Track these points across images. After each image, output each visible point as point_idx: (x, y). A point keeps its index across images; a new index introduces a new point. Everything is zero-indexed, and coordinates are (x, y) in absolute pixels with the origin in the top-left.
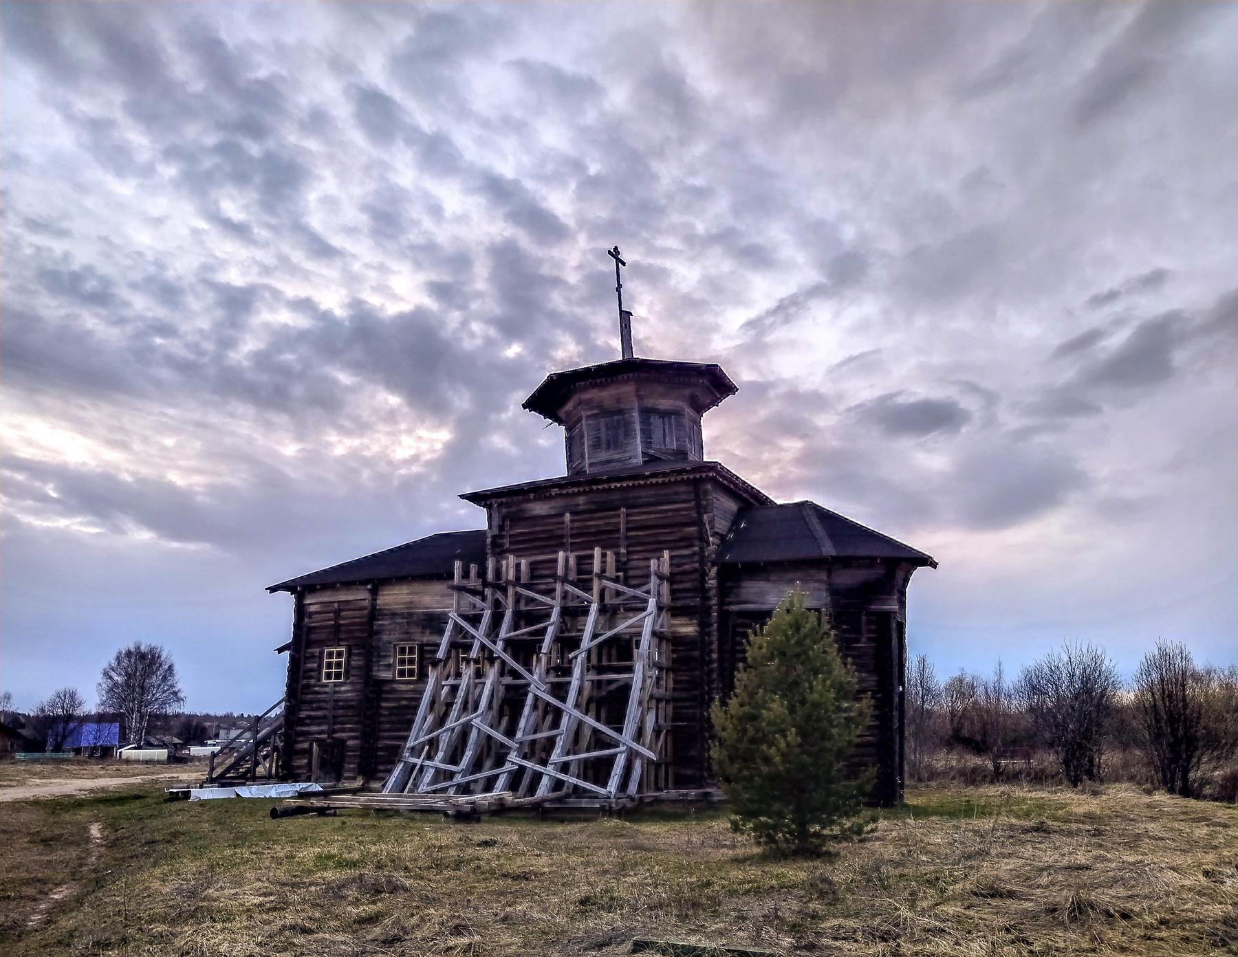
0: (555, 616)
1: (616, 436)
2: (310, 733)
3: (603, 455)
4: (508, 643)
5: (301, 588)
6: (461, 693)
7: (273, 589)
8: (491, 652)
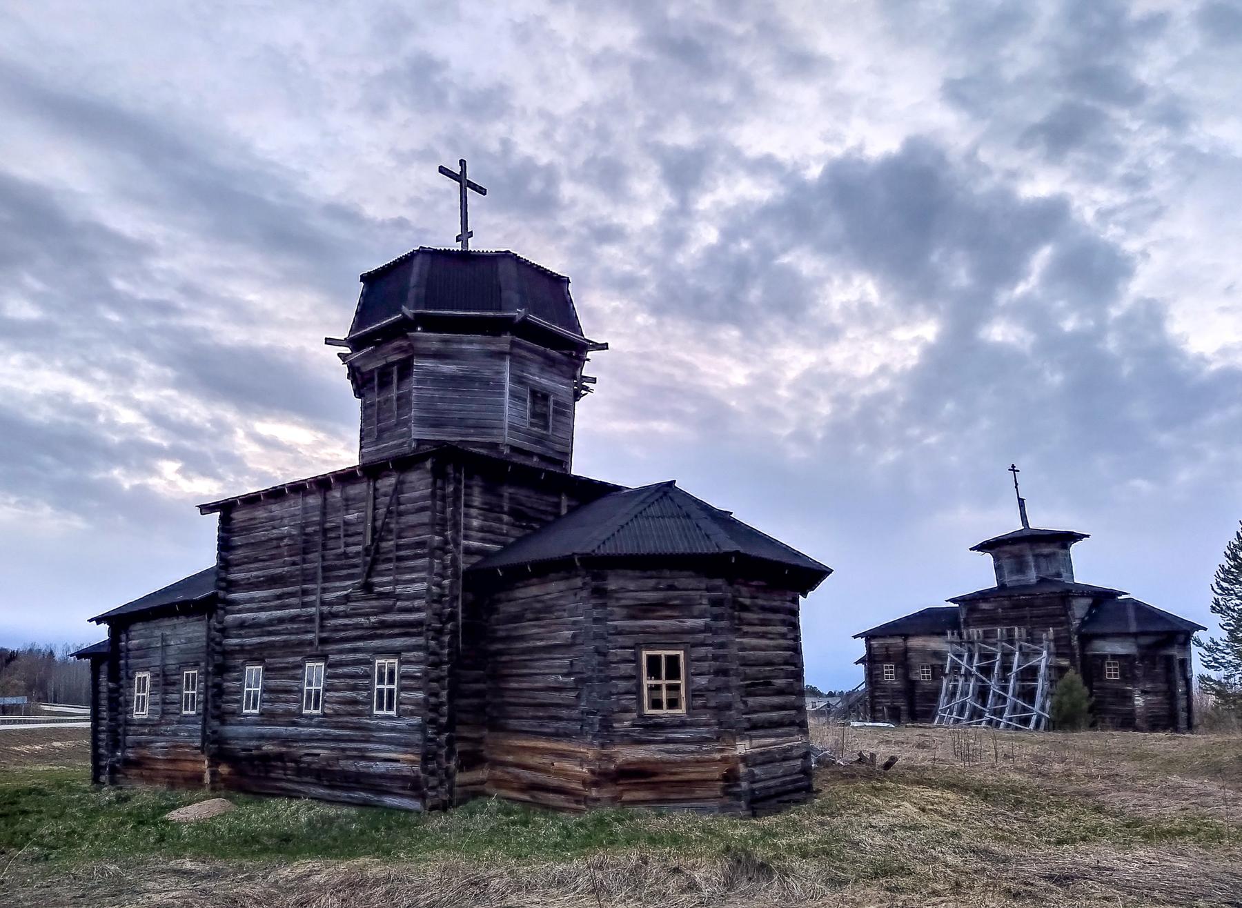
0: (998, 657)
1: (1021, 568)
2: (882, 702)
3: (1015, 578)
4: (980, 669)
5: (869, 636)
6: (960, 688)
7: (855, 637)
8: (970, 672)
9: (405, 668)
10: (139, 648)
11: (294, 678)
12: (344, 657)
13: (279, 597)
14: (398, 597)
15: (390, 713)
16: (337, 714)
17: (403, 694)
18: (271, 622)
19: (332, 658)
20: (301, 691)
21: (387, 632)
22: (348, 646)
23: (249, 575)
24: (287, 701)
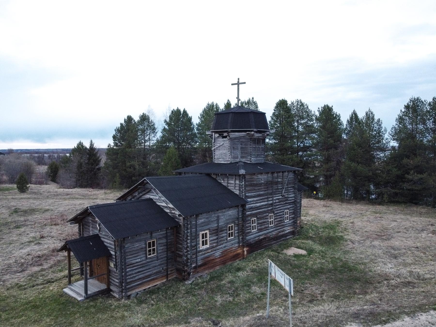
9: (290, 211)
10: (202, 223)
11: (266, 219)
12: (278, 212)
13: (261, 199)
14: (288, 198)
15: (288, 221)
16: (277, 224)
17: (290, 216)
18: (260, 206)
19: (276, 212)
20: (268, 221)
21: (286, 205)
22: (279, 209)
23: (252, 194)
24: (264, 225)
